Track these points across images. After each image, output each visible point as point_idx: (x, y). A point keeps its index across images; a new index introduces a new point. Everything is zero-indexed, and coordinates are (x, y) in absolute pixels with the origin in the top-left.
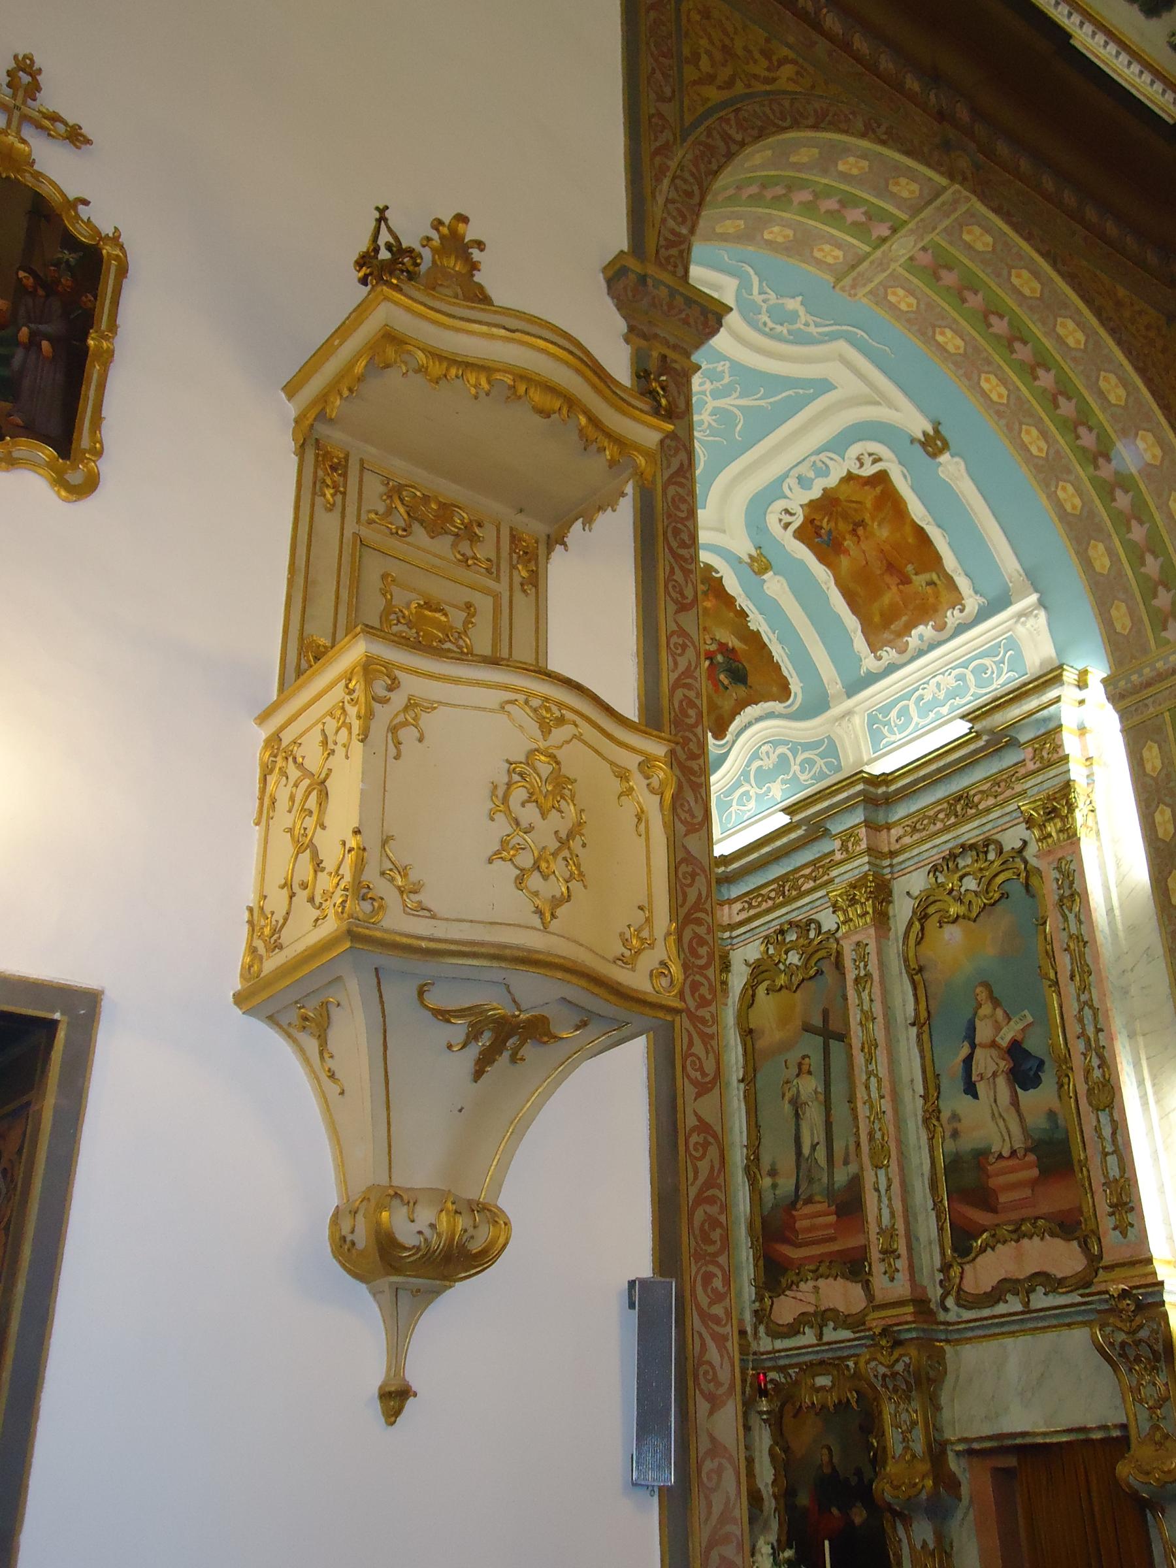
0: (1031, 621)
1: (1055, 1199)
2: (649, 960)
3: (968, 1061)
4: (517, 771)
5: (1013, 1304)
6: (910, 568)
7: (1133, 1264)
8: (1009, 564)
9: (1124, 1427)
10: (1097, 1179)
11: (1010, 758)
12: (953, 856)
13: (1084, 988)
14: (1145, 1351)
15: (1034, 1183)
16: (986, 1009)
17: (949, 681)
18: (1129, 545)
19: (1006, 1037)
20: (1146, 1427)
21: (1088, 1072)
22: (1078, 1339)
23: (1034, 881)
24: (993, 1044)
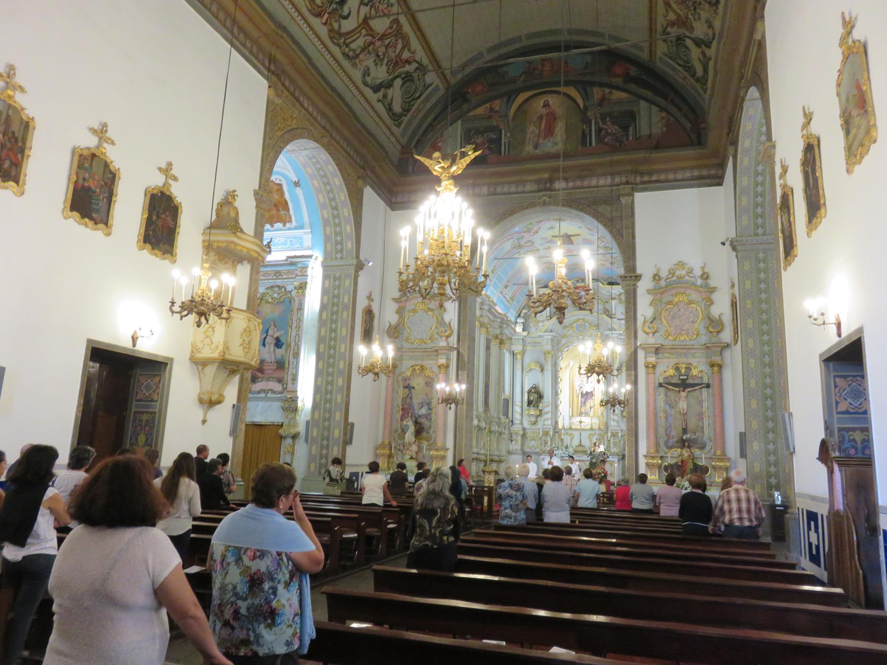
0: (307, 236)
1: (278, 374)
2: (255, 359)
3: (265, 338)
4: (245, 330)
5: (263, 395)
6: (281, 208)
7: (293, 392)
8: (306, 219)
9: (283, 423)
10: (290, 373)
11: (293, 268)
12: (272, 287)
13: (298, 331)
14: (291, 409)
15: (275, 370)
16: (272, 327)
17: (283, 240)
18: (335, 232)
19: (276, 335)
20: (287, 423)
21: (294, 350)
22: (277, 405)
23: (292, 300)
24: (272, 336)
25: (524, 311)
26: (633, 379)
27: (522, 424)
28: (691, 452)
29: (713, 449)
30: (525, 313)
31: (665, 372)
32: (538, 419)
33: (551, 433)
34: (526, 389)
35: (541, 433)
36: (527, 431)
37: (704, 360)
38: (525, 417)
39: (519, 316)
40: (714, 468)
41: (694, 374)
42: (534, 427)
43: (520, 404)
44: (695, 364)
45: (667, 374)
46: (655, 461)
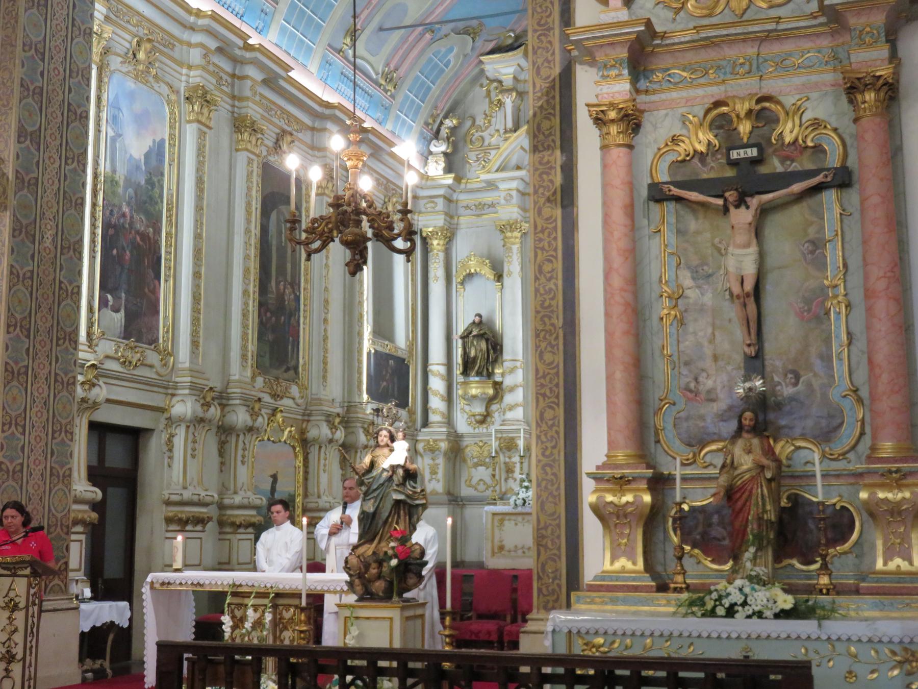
25: (448, 123)
26: (558, 179)
27: (449, 420)
28: (769, 452)
29: (867, 441)
30: (453, 130)
31: (675, 140)
32: (494, 407)
33: (521, 443)
34: (460, 328)
35: (494, 444)
36: (467, 441)
37: (829, 77)
38: (460, 405)
39: (437, 135)
40: (872, 511)
41: (788, 139)
42: (482, 429)
43: (442, 370)
44: (789, 101)
45: (684, 148)
46: (629, 498)
